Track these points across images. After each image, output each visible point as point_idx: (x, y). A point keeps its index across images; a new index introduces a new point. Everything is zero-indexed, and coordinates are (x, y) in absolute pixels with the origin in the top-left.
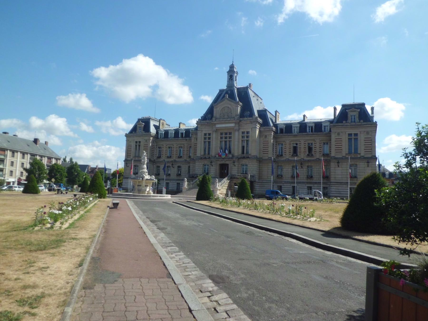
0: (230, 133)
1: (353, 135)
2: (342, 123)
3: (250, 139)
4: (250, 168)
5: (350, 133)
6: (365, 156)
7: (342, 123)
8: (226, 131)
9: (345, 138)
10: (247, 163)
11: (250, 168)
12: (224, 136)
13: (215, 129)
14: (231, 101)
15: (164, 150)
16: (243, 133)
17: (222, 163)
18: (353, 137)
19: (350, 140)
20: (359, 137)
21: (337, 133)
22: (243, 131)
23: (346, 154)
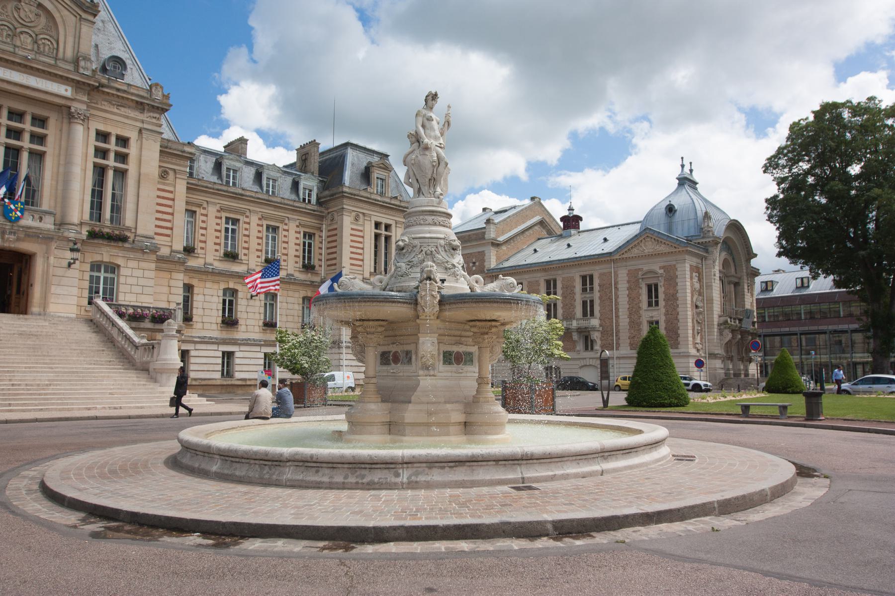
0: (41, 121)
3: (131, 167)
4: (130, 280)
5: (379, 220)
8: (19, 106)
10: (120, 261)
11: (130, 280)
16: (103, 136)
19: (377, 236)
21: (354, 214)
22: (102, 128)
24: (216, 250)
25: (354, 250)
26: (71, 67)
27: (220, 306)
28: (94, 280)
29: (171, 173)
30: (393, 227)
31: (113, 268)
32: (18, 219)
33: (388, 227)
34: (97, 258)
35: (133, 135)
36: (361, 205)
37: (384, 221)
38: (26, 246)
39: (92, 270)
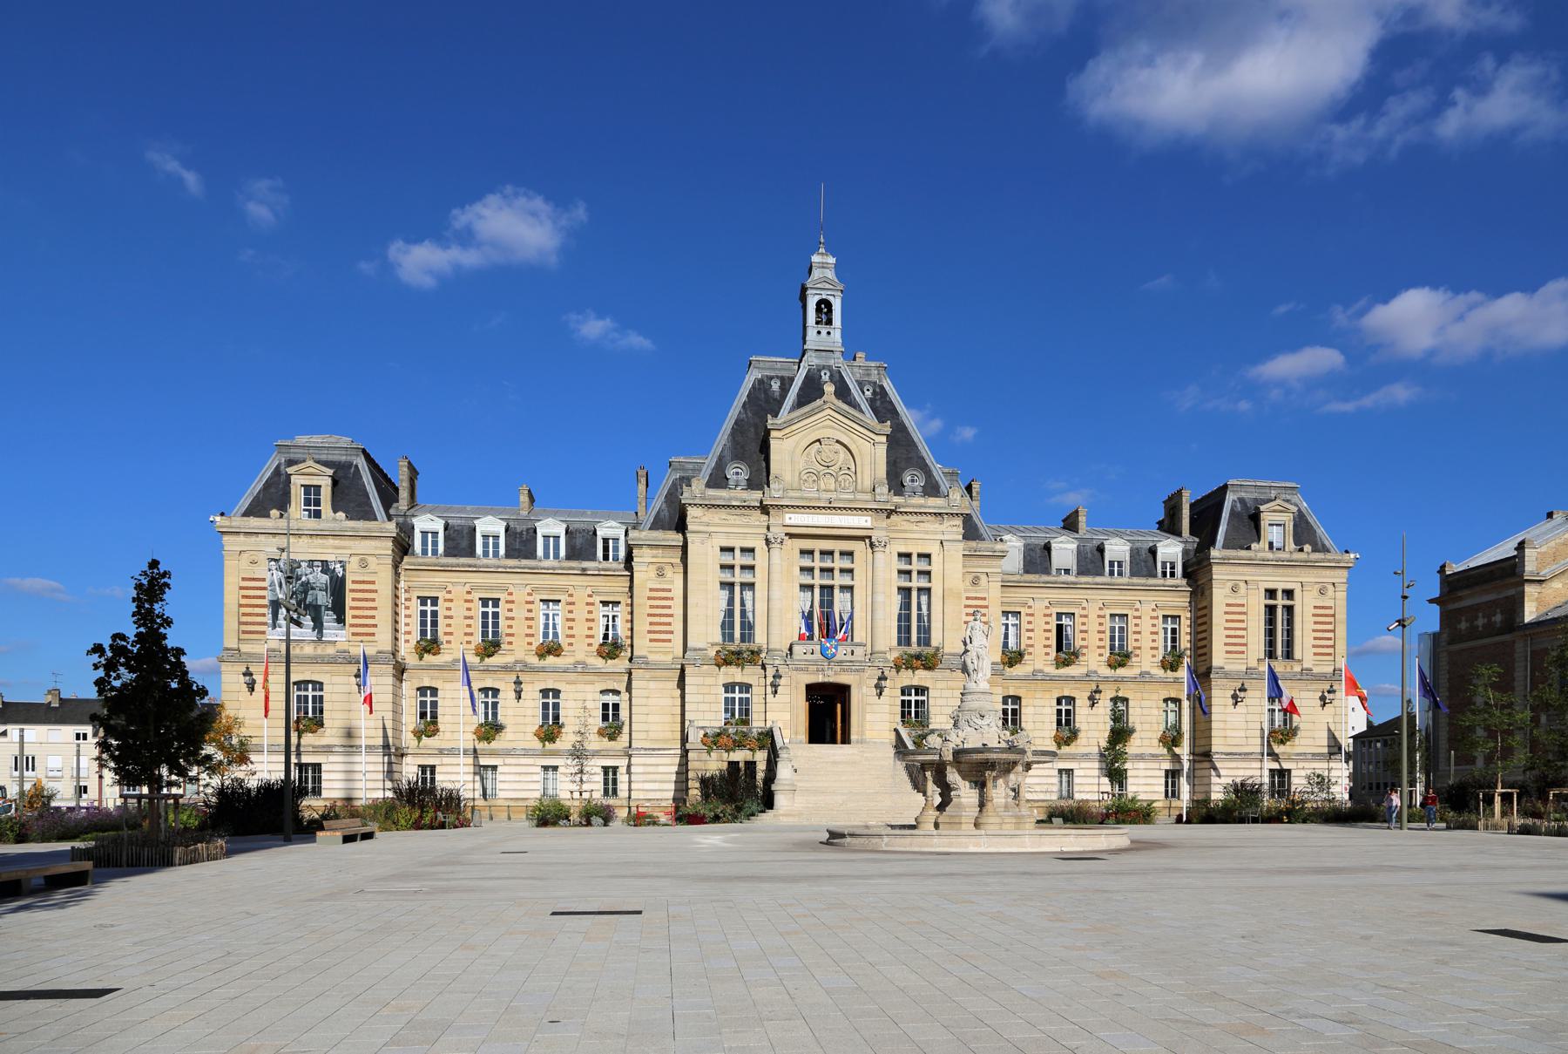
1: (1279, 594)
2: (1249, 548)
4: (940, 702)
5: (1271, 586)
6: (1316, 670)
7: (1249, 548)
9: (1257, 604)
11: (940, 702)
13: (777, 532)
15: (520, 613)
16: (906, 556)
17: (820, 679)
18: (1280, 601)
19: (1271, 610)
20: (1297, 603)
22: (903, 550)
26: (869, 497)
27: (1055, 718)
28: (905, 704)
29: (984, 577)
30: (1297, 594)
31: (921, 690)
32: (834, 655)
33: (1289, 594)
34: (907, 683)
35: (933, 549)
36: (1241, 569)
37: (1280, 586)
38: (843, 679)
39: (903, 693)
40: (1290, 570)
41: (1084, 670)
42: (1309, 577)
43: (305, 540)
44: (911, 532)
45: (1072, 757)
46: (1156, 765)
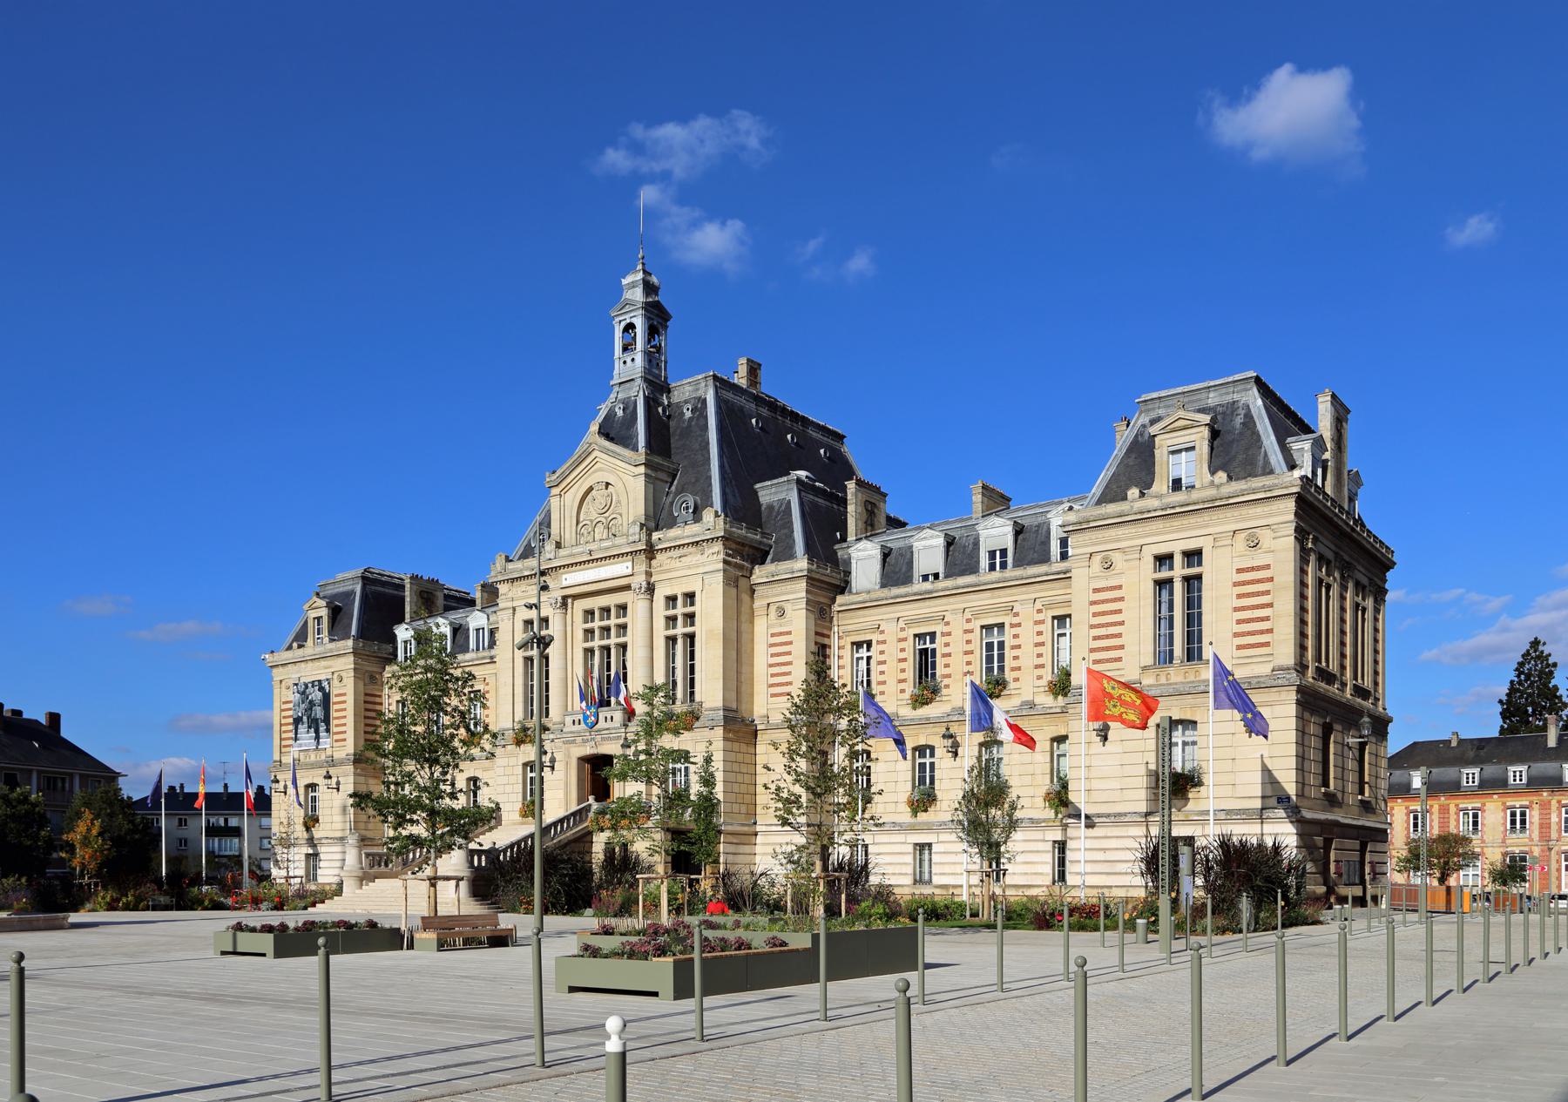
3: (697, 629)
5: (1163, 549)
9: (1138, 580)
12: (597, 624)
14: (615, 455)
16: (671, 600)
19: (1163, 584)
23: (1145, 668)
24: (903, 691)
25: (1102, 632)
36: (1112, 532)
37: (1177, 548)
40: (1192, 520)
41: (947, 708)
42: (1224, 522)
43: (310, 664)
44: (675, 570)
45: (928, 827)
46: (1038, 835)
